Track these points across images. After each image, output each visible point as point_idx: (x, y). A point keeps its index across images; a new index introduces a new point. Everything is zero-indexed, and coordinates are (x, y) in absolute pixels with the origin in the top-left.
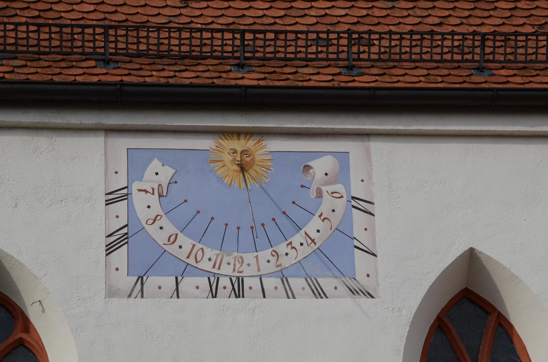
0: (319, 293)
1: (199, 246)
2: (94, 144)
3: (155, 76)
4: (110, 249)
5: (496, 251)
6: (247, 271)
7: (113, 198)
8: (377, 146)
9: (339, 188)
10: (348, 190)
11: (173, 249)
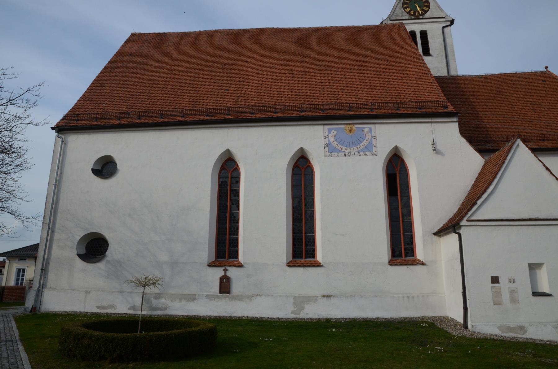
0: (366, 155)
2: (321, 127)
3: (332, 113)
5: (400, 145)
7: (325, 138)
8: (377, 126)
9: (370, 134)
11: (337, 147)
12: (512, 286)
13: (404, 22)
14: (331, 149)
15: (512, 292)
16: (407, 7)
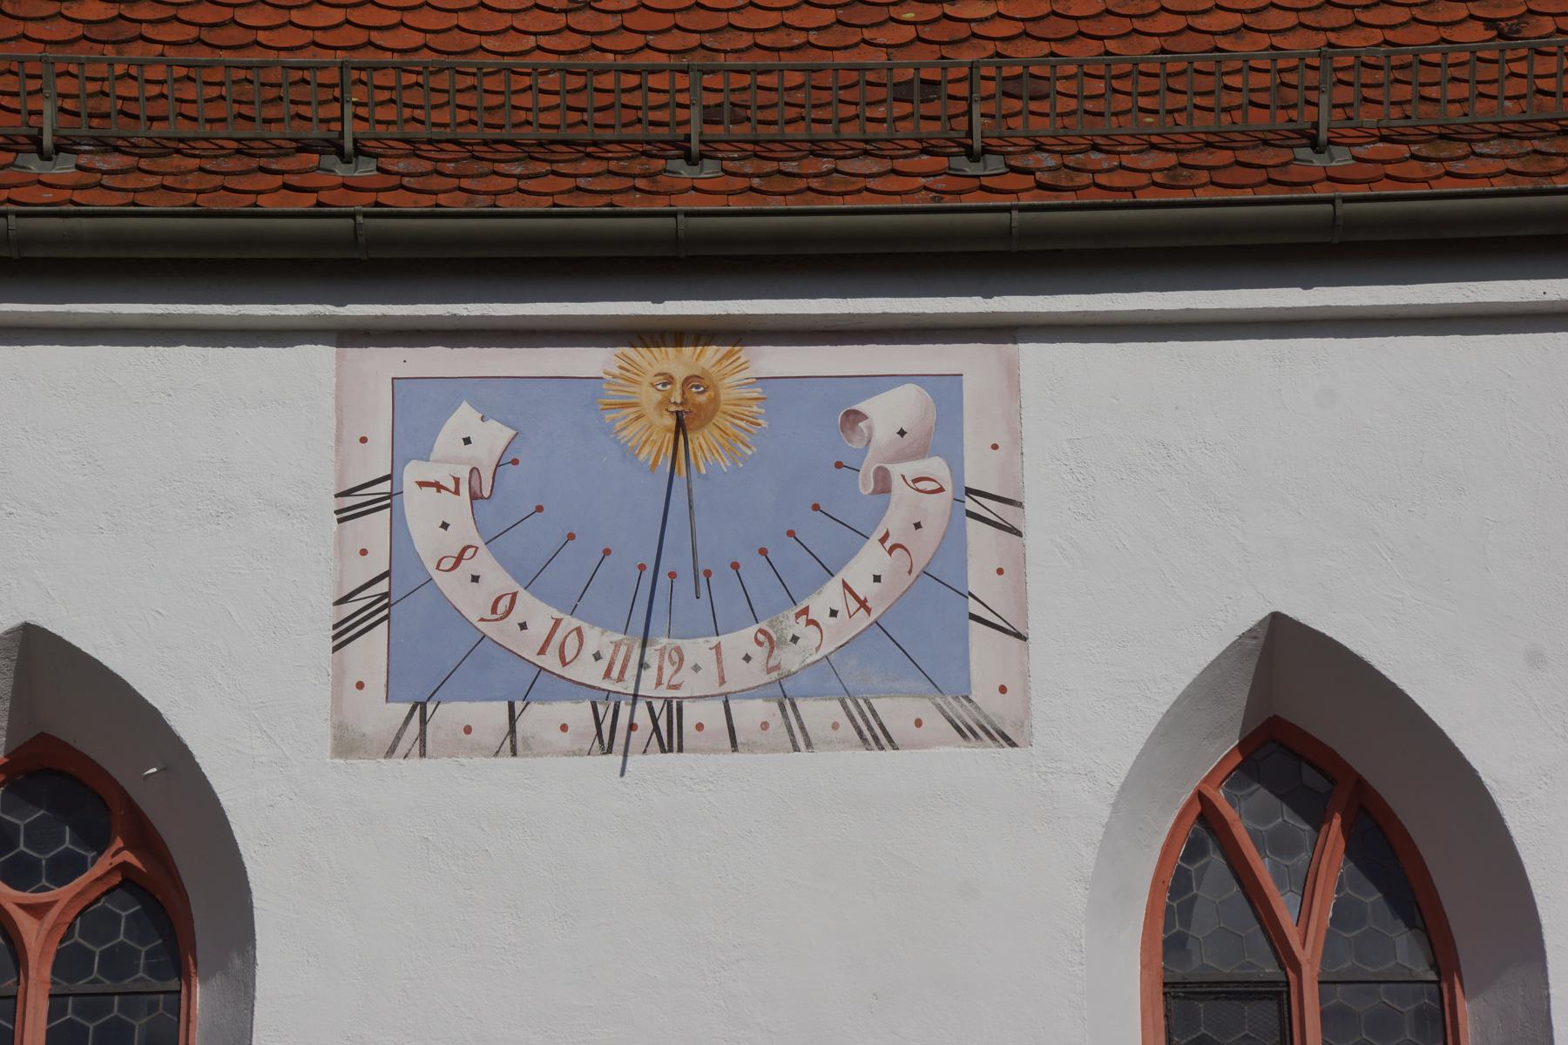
0: (876, 737)
1: (569, 622)
6: (692, 684)
9: (936, 467)
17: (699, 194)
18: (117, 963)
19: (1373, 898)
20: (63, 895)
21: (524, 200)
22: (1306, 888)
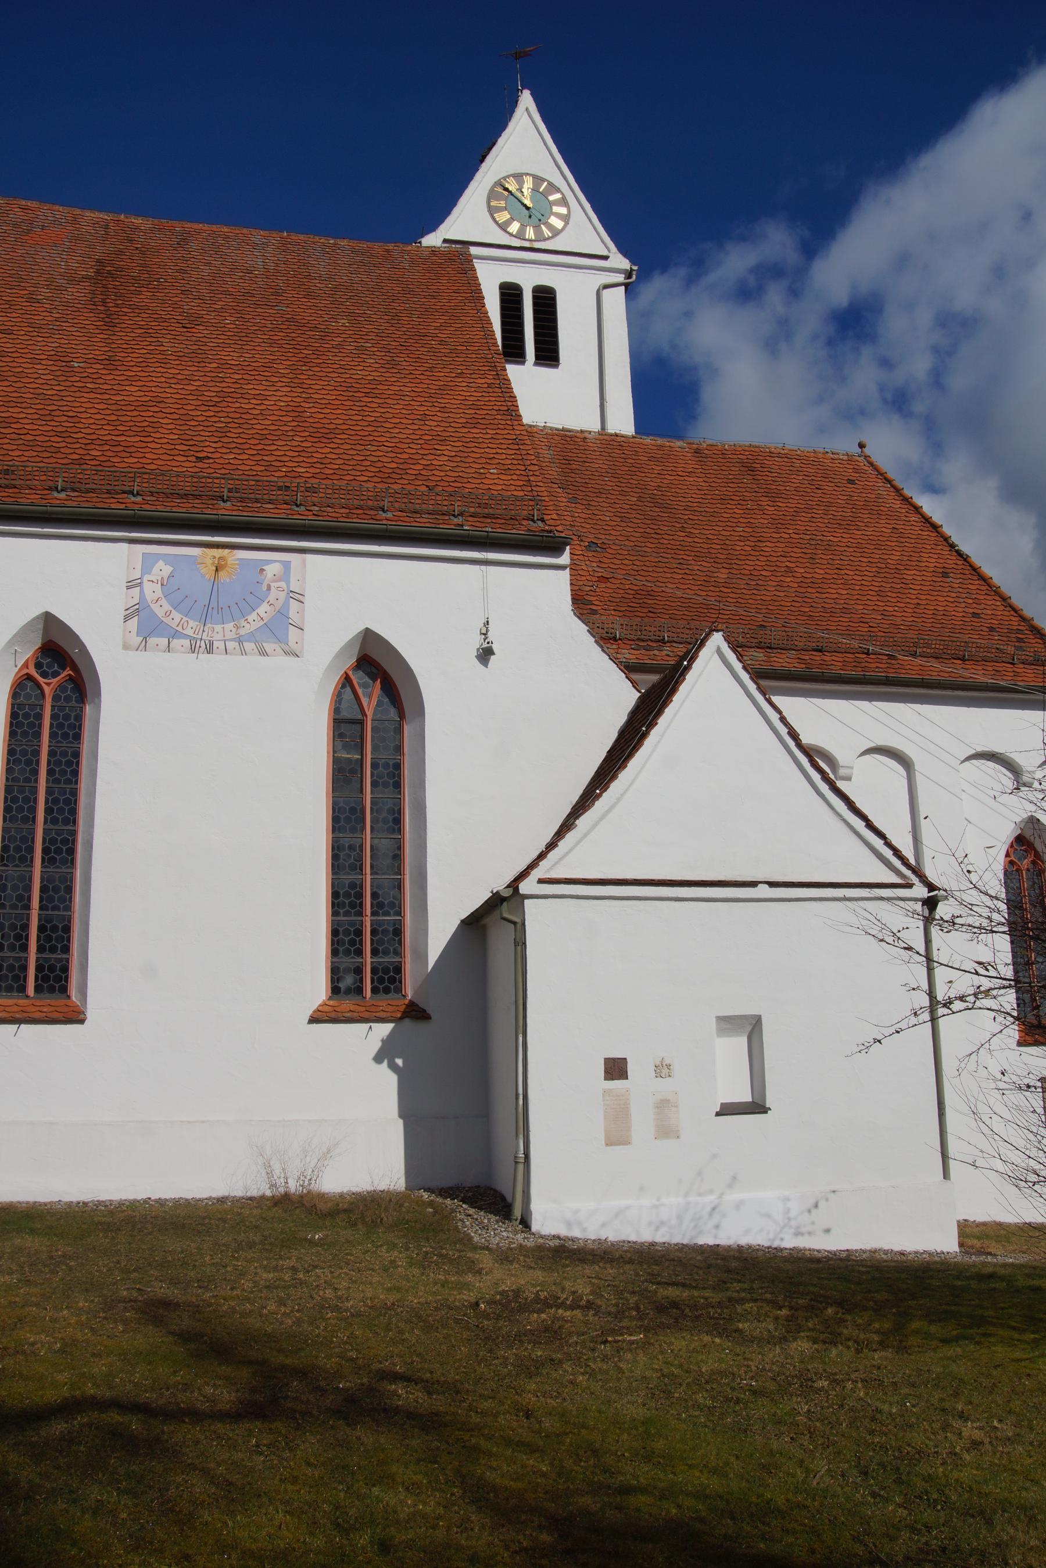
0: (263, 653)
1: (185, 619)
4: (126, 619)
6: (216, 637)
9: (283, 584)
10: (288, 587)
12: (664, 1087)
13: (474, 250)
14: (146, 626)
15: (663, 1106)
16: (499, 209)
17: (225, 510)
18: (68, 699)
19: (386, 700)
20: (54, 681)
21: (180, 509)
22: (370, 696)
